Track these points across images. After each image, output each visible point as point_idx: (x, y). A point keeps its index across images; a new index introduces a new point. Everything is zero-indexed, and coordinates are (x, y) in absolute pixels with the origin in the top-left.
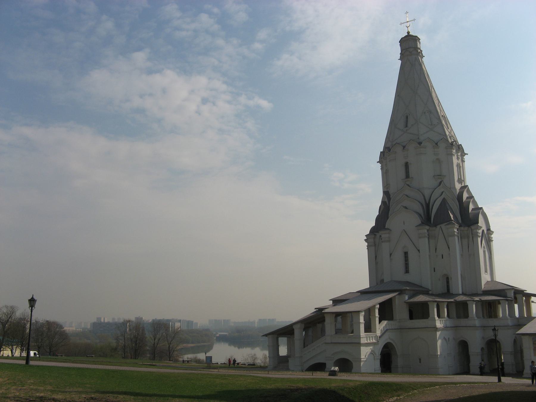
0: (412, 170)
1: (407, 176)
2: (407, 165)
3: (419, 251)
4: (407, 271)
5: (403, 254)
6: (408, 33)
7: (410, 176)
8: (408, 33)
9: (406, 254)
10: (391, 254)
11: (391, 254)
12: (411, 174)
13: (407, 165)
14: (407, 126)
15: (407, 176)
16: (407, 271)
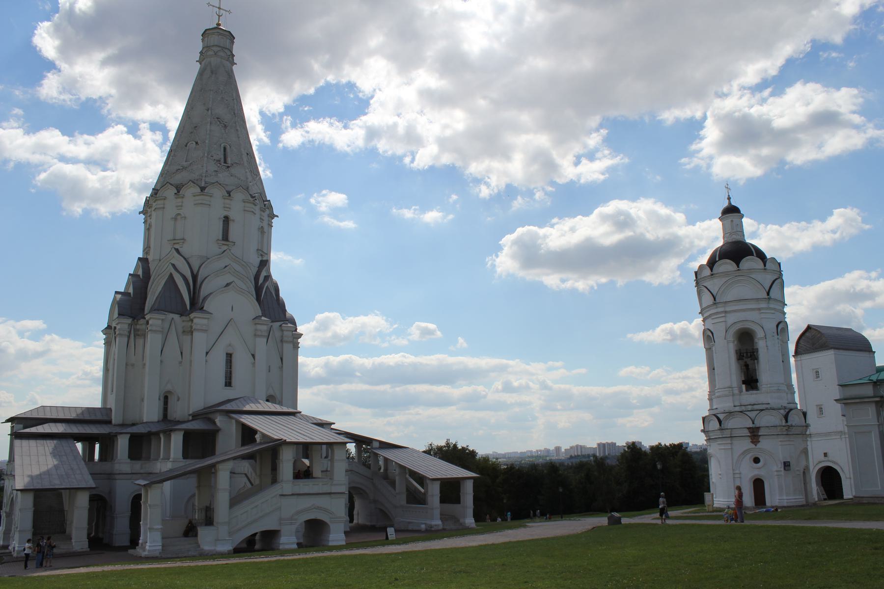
0: (234, 232)
1: (225, 237)
2: (226, 220)
3: (253, 356)
4: (228, 384)
5: (223, 358)
6: (219, 25)
7: (230, 239)
8: (219, 25)
9: (229, 356)
10: (207, 353)
11: (207, 353)
12: (231, 237)
13: (226, 220)
14: (225, 162)
15: (225, 237)
16: (228, 384)
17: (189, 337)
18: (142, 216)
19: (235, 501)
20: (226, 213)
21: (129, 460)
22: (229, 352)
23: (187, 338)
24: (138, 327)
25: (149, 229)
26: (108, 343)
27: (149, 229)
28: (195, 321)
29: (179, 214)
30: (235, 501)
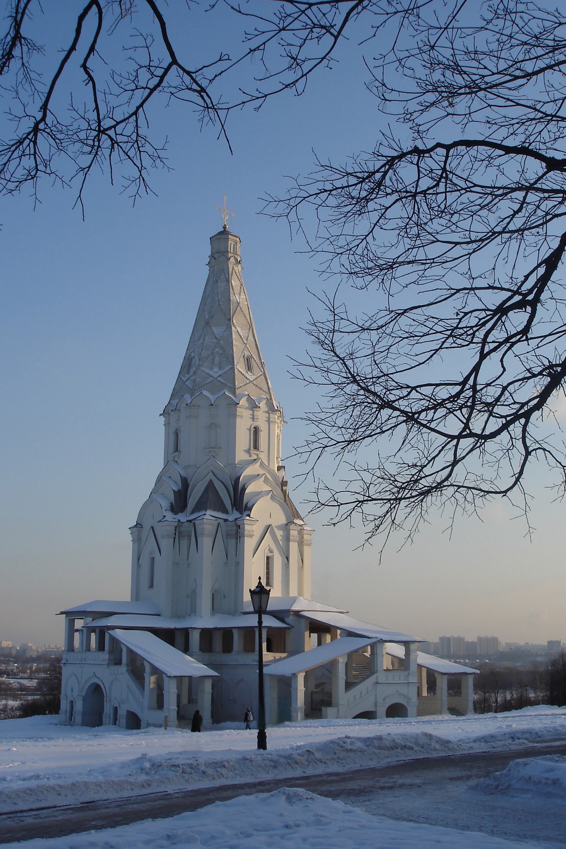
2: (256, 430)
3: (288, 558)
8: (225, 227)
9: (268, 558)
17: (233, 541)
18: (162, 419)
19: (349, 685)
20: (256, 424)
21: (200, 653)
22: (270, 554)
23: (232, 542)
24: (182, 529)
25: (177, 434)
26: (138, 540)
27: (177, 434)
28: (247, 527)
29: (212, 424)
30: (349, 685)
